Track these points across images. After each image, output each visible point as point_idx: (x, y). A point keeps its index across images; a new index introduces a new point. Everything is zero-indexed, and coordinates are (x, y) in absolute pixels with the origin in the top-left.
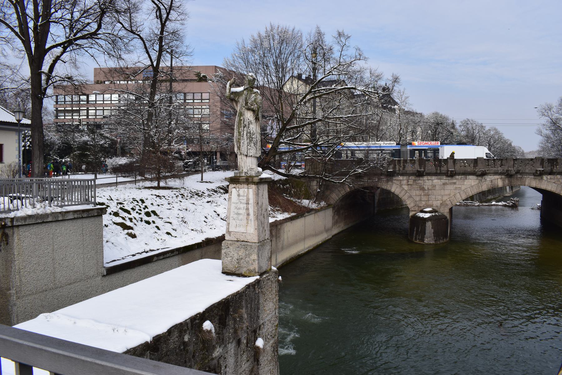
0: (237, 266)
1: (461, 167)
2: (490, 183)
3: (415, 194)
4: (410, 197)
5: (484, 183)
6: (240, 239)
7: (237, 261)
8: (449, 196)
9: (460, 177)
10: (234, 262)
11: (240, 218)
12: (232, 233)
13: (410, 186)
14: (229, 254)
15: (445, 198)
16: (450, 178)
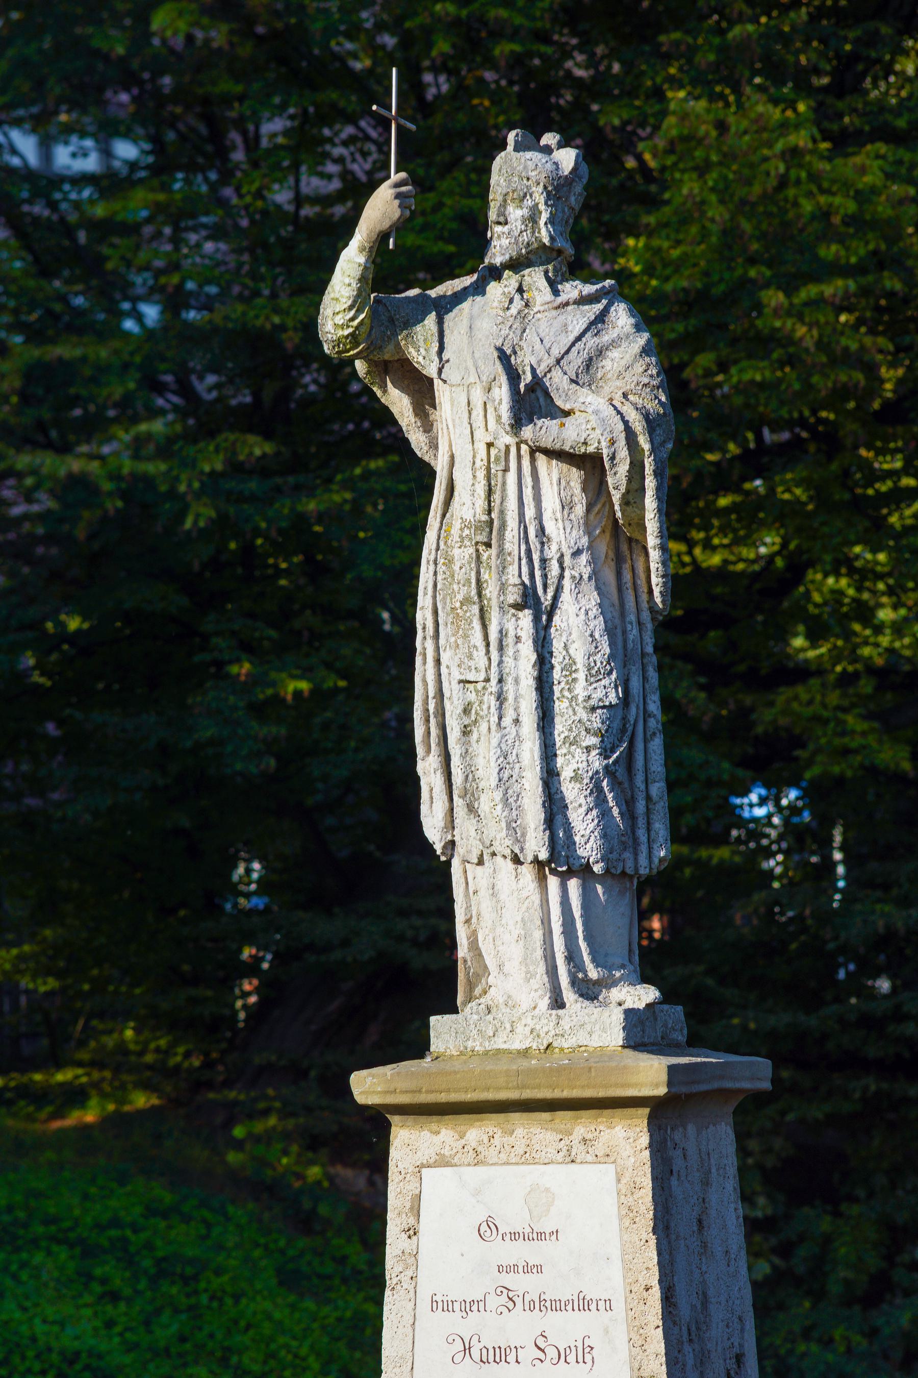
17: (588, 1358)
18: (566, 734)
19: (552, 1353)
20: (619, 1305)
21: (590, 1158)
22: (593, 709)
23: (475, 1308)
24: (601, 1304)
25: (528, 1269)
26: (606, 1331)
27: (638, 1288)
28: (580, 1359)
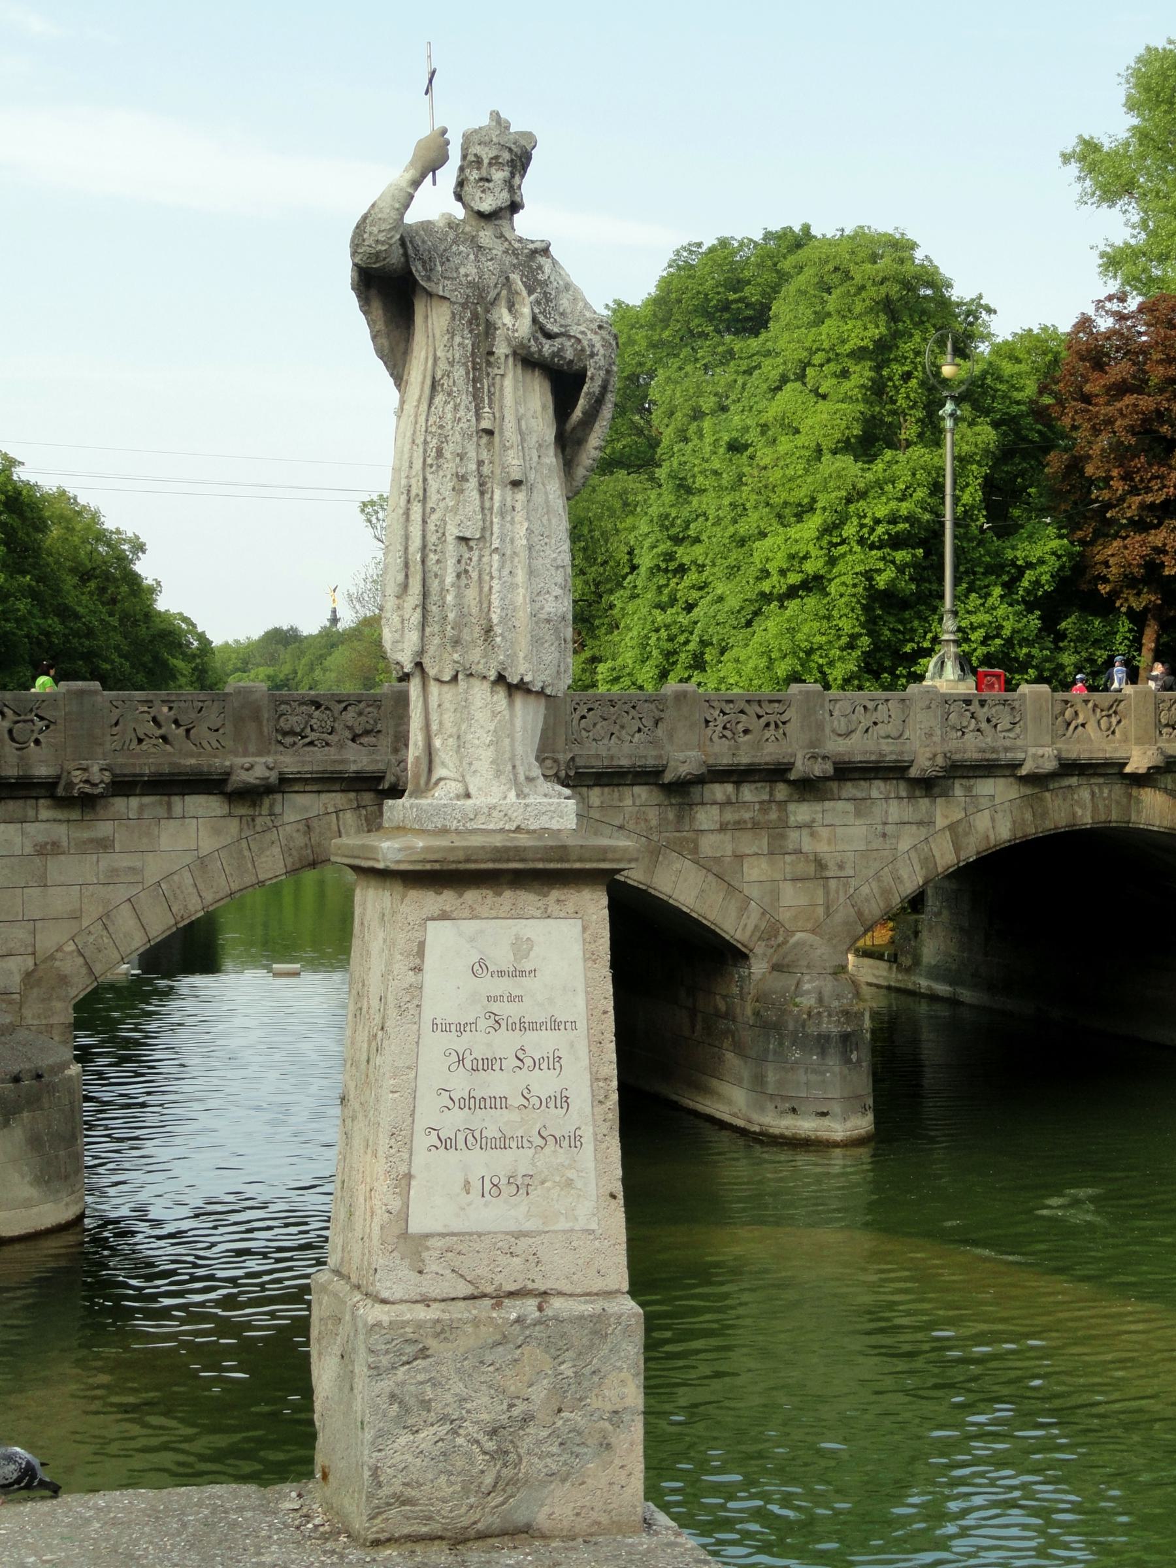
0: (489, 1480)
1: (140, 741)
2: (300, 840)
5: (269, 837)
6: (498, 1279)
7: (491, 1446)
9: (134, 802)
10: (469, 1455)
12: (431, 1243)
14: (426, 1405)
15: (48, 940)
16: (75, 815)
17: (557, 1065)
19: (528, 1062)
20: (582, 1025)
21: (562, 915)
23: (468, 1029)
25: (511, 999)
26: (572, 1045)
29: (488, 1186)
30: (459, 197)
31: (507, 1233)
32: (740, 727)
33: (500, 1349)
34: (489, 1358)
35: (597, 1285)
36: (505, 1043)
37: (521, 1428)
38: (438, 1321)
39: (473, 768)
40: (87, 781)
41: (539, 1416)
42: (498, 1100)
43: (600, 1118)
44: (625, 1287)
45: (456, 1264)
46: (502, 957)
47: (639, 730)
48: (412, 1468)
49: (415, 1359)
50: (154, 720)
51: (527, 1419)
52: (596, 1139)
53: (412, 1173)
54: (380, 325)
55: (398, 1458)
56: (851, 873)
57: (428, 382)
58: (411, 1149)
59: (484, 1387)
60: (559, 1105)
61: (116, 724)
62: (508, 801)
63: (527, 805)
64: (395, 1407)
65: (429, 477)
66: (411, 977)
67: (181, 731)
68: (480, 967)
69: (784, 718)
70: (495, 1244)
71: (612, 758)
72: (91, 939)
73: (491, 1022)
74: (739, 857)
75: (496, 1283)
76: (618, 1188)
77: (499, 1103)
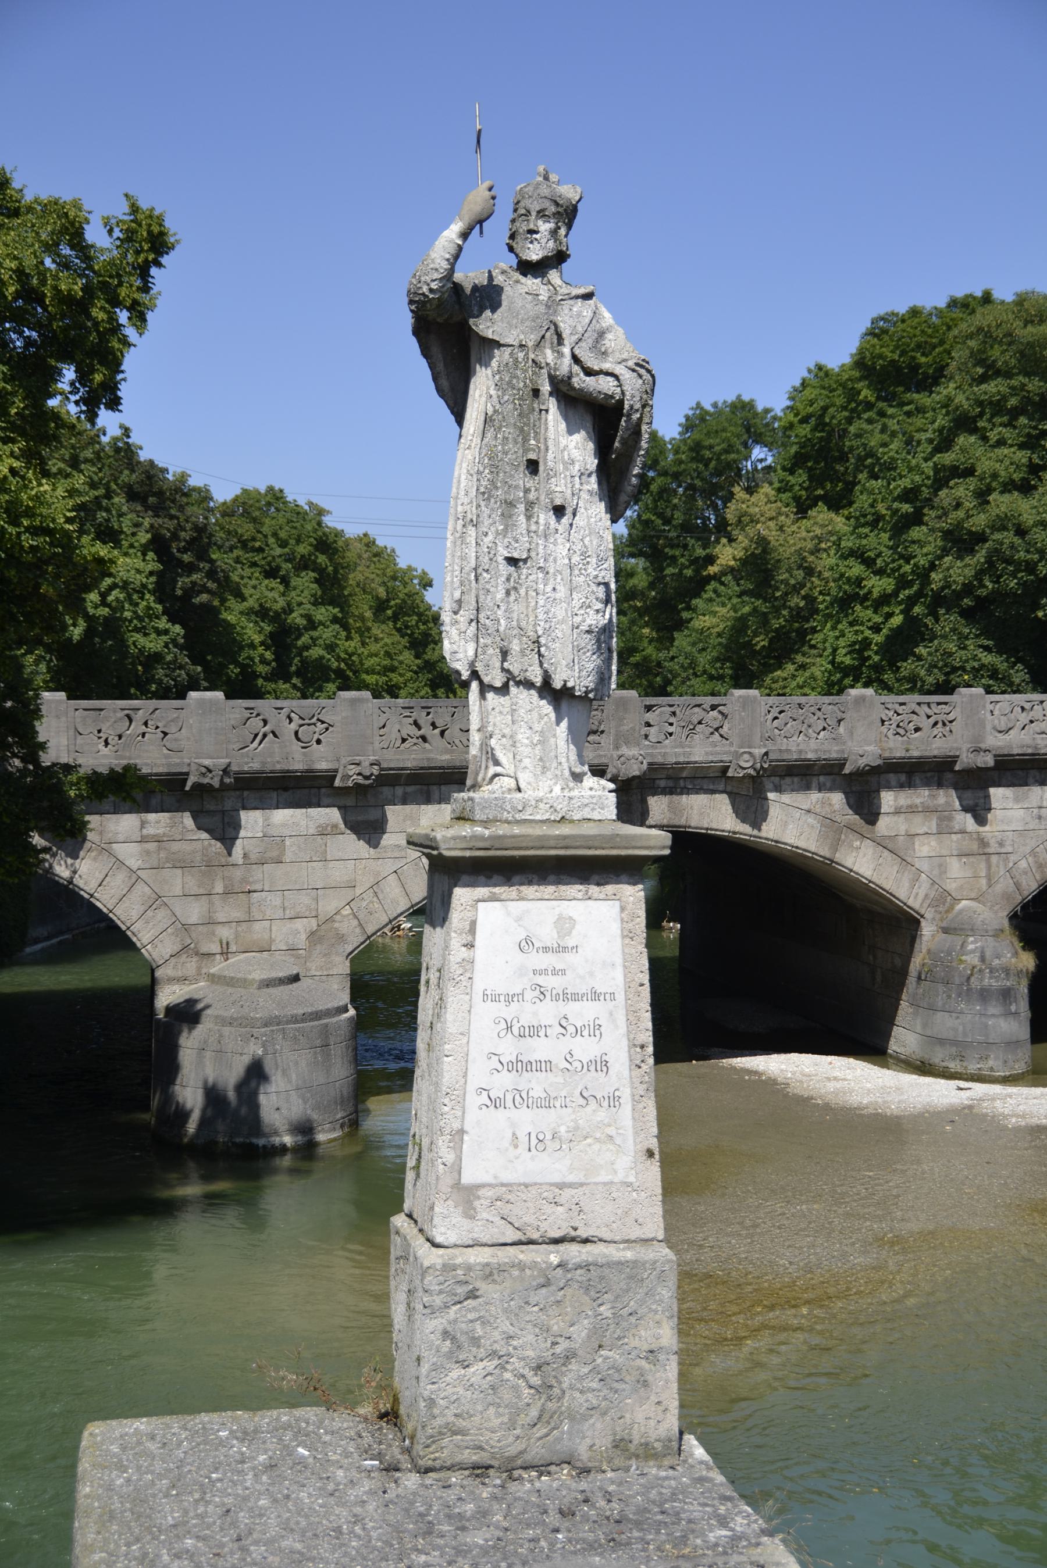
0: (534, 1413)
1: (404, 740)
3: (178, 891)
4: (157, 901)
6: (544, 1226)
7: (536, 1381)
8: (349, 894)
10: (515, 1388)
11: (537, 1092)
12: (481, 1192)
13: (152, 846)
14: (475, 1341)
15: (329, 905)
17: (597, 1033)
18: (584, 600)
19: (571, 1029)
20: (620, 997)
21: (602, 896)
22: (599, 584)
23: (515, 999)
24: (608, 996)
25: (555, 972)
26: (611, 1014)
27: (634, 985)
28: (592, 1033)
29: (534, 1141)
30: (511, 249)
31: (552, 1185)
32: (911, 726)
33: (544, 1291)
34: (533, 1300)
35: (636, 1233)
36: (547, 1012)
37: (564, 1365)
38: (487, 1264)
39: (523, 765)
40: (359, 774)
41: (580, 1353)
42: (543, 1064)
43: (637, 1081)
44: (661, 1235)
45: (505, 1212)
46: (547, 935)
47: (824, 729)
48: (463, 1401)
49: (466, 1299)
50: (416, 723)
51: (569, 1357)
52: (633, 1100)
53: (466, 1128)
54: (441, 366)
55: (450, 1390)
56: (1009, 849)
57: (483, 419)
58: (464, 1107)
59: (529, 1326)
60: (599, 1068)
61: (384, 727)
62: (553, 794)
63: (570, 798)
64: (448, 1343)
65: (483, 504)
66: (464, 952)
67: (437, 731)
68: (526, 944)
69: (951, 717)
70: (541, 1194)
71: (800, 752)
72: (364, 904)
73: (537, 993)
74: (912, 836)
75: (542, 1230)
76: (654, 1144)
77: (546, 1066)
